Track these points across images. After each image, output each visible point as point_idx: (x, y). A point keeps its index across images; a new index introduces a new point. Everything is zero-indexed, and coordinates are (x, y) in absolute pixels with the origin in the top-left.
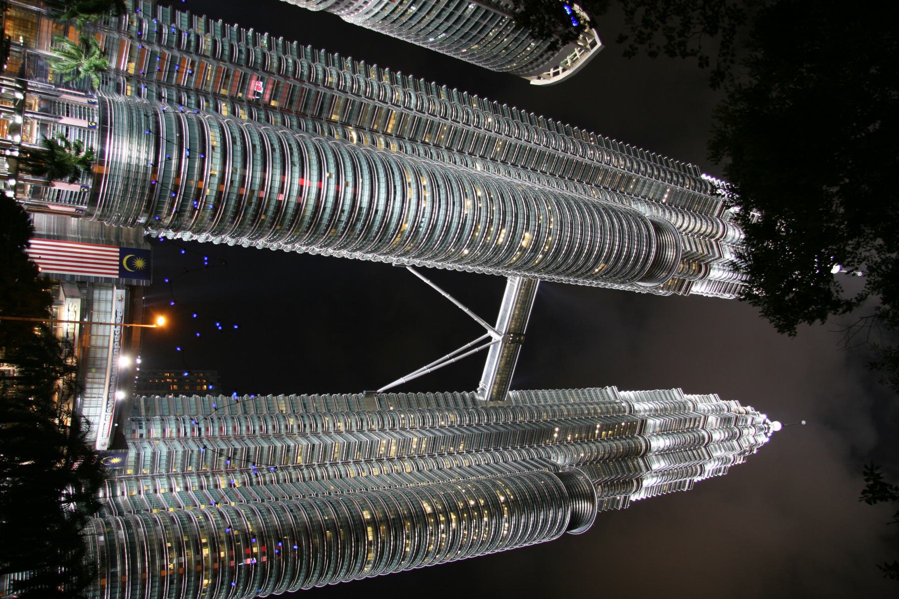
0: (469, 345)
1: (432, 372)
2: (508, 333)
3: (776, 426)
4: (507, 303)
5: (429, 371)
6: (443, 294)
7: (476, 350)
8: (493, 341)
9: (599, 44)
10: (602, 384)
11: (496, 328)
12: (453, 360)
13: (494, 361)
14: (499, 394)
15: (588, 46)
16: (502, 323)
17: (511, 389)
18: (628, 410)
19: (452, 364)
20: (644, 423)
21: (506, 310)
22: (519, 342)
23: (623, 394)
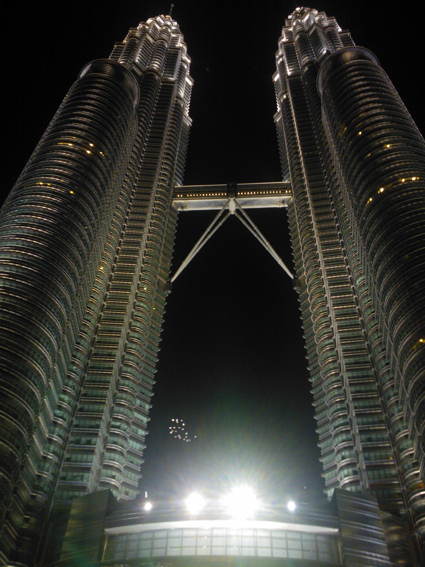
0: (244, 223)
1: (268, 240)
2: (227, 197)
4: (203, 205)
5: (267, 244)
7: (244, 214)
8: (237, 208)
12: (255, 228)
19: (259, 228)
21: (209, 204)
22: (236, 187)
23: (279, 109)
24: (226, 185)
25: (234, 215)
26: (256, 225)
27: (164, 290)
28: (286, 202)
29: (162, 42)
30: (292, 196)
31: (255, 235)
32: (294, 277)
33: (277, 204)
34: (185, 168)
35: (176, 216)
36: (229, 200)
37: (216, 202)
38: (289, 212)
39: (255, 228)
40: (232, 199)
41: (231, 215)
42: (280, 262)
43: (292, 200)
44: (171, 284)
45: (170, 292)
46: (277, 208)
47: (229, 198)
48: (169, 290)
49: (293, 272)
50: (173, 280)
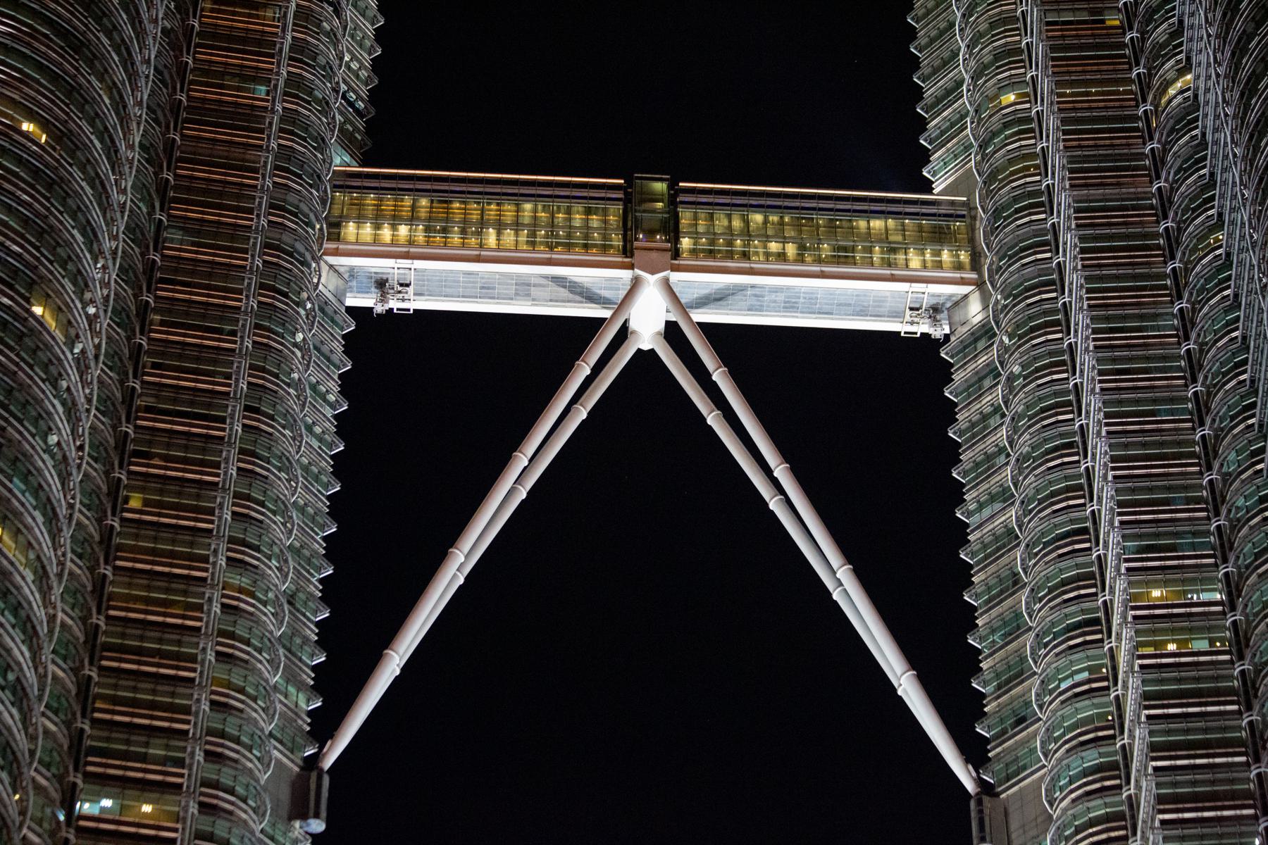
0: (713, 419)
5: (844, 574)
7: (719, 377)
11: (606, 314)
12: (781, 472)
13: (776, 290)
16: (590, 297)
17: (927, 186)
21: (523, 288)
26: (786, 454)
27: (291, 818)
28: (943, 316)
30: (980, 285)
31: (774, 505)
32: (980, 782)
33: (896, 315)
34: (380, 34)
35: (338, 347)
36: (636, 283)
38: (959, 377)
43: (975, 312)
44: (326, 781)
45: (318, 826)
48: (317, 816)
49: (974, 751)
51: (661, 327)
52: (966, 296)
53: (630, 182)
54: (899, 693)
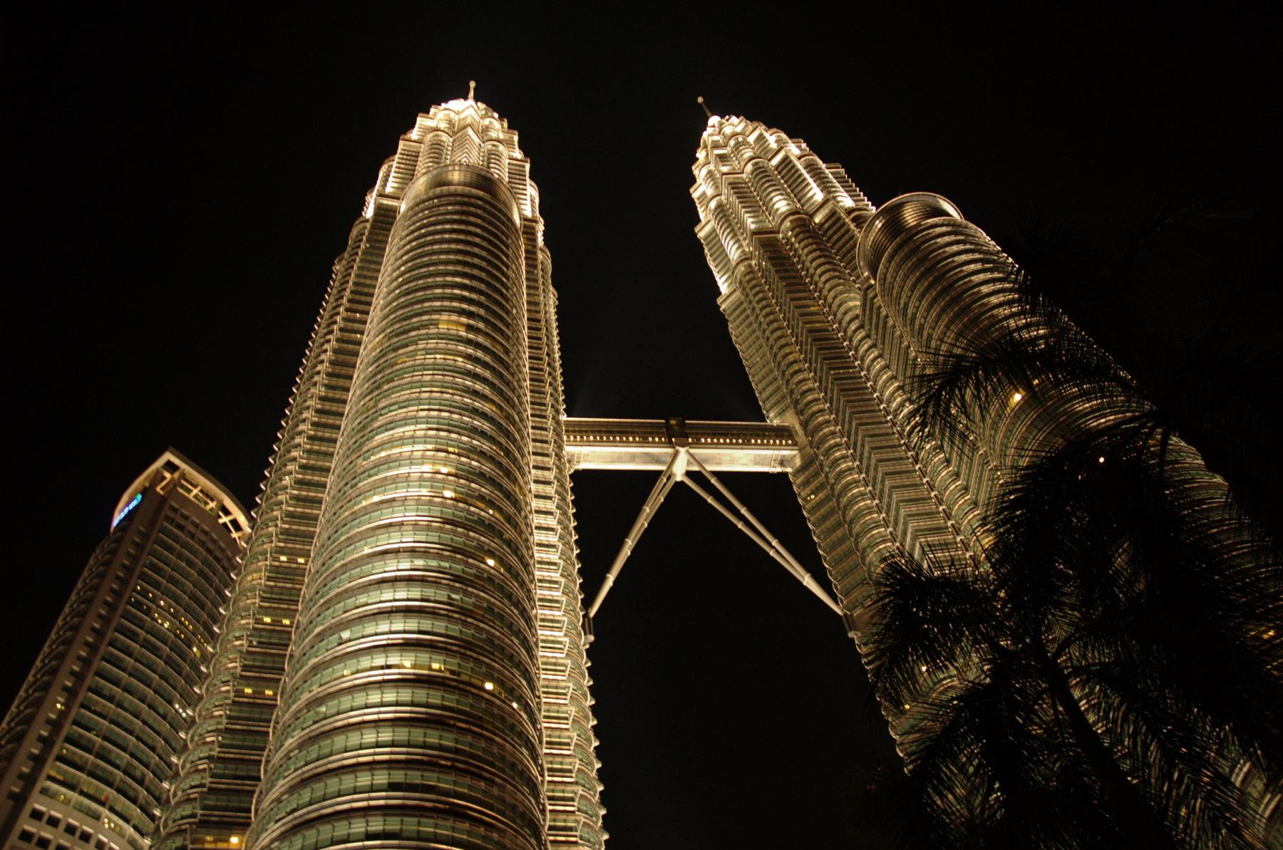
1: (775, 536)
2: (670, 444)
3: (714, 120)
5: (774, 543)
6: (626, 552)
7: (713, 481)
9: (168, 456)
10: (721, 320)
12: (743, 511)
14: (782, 434)
15: (176, 475)
16: (656, 460)
18: (746, 263)
19: (750, 510)
20: (754, 233)
21: (633, 458)
22: (682, 425)
24: (663, 421)
25: (682, 483)
29: (494, 145)
31: (740, 525)
36: (676, 454)
37: (647, 454)
39: (743, 511)
40: (682, 450)
41: (676, 482)
42: (808, 581)
46: (766, 474)
47: (678, 448)
48: (590, 633)
50: (593, 612)
51: (684, 471)
52: (795, 456)
53: (667, 421)
54: (805, 584)
